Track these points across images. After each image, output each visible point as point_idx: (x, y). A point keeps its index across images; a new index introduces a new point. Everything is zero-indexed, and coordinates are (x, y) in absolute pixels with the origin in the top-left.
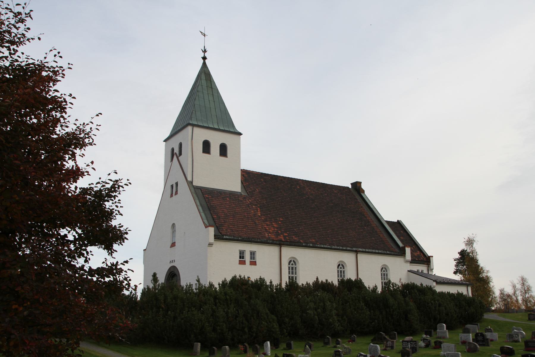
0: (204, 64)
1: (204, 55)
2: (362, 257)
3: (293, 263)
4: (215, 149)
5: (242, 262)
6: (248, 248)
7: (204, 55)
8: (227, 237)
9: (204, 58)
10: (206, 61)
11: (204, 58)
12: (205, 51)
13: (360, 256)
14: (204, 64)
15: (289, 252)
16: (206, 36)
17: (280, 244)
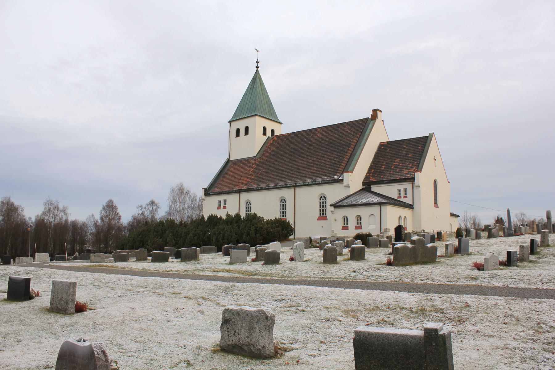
0: (257, 70)
1: (257, 65)
2: (301, 191)
3: (248, 203)
4: (242, 132)
5: (219, 208)
6: (222, 198)
7: (257, 65)
8: (212, 193)
9: (257, 67)
10: (259, 69)
11: (257, 67)
12: (258, 63)
13: (298, 190)
14: (257, 70)
15: (245, 197)
16: (259, 52)
17: (240, 192)
